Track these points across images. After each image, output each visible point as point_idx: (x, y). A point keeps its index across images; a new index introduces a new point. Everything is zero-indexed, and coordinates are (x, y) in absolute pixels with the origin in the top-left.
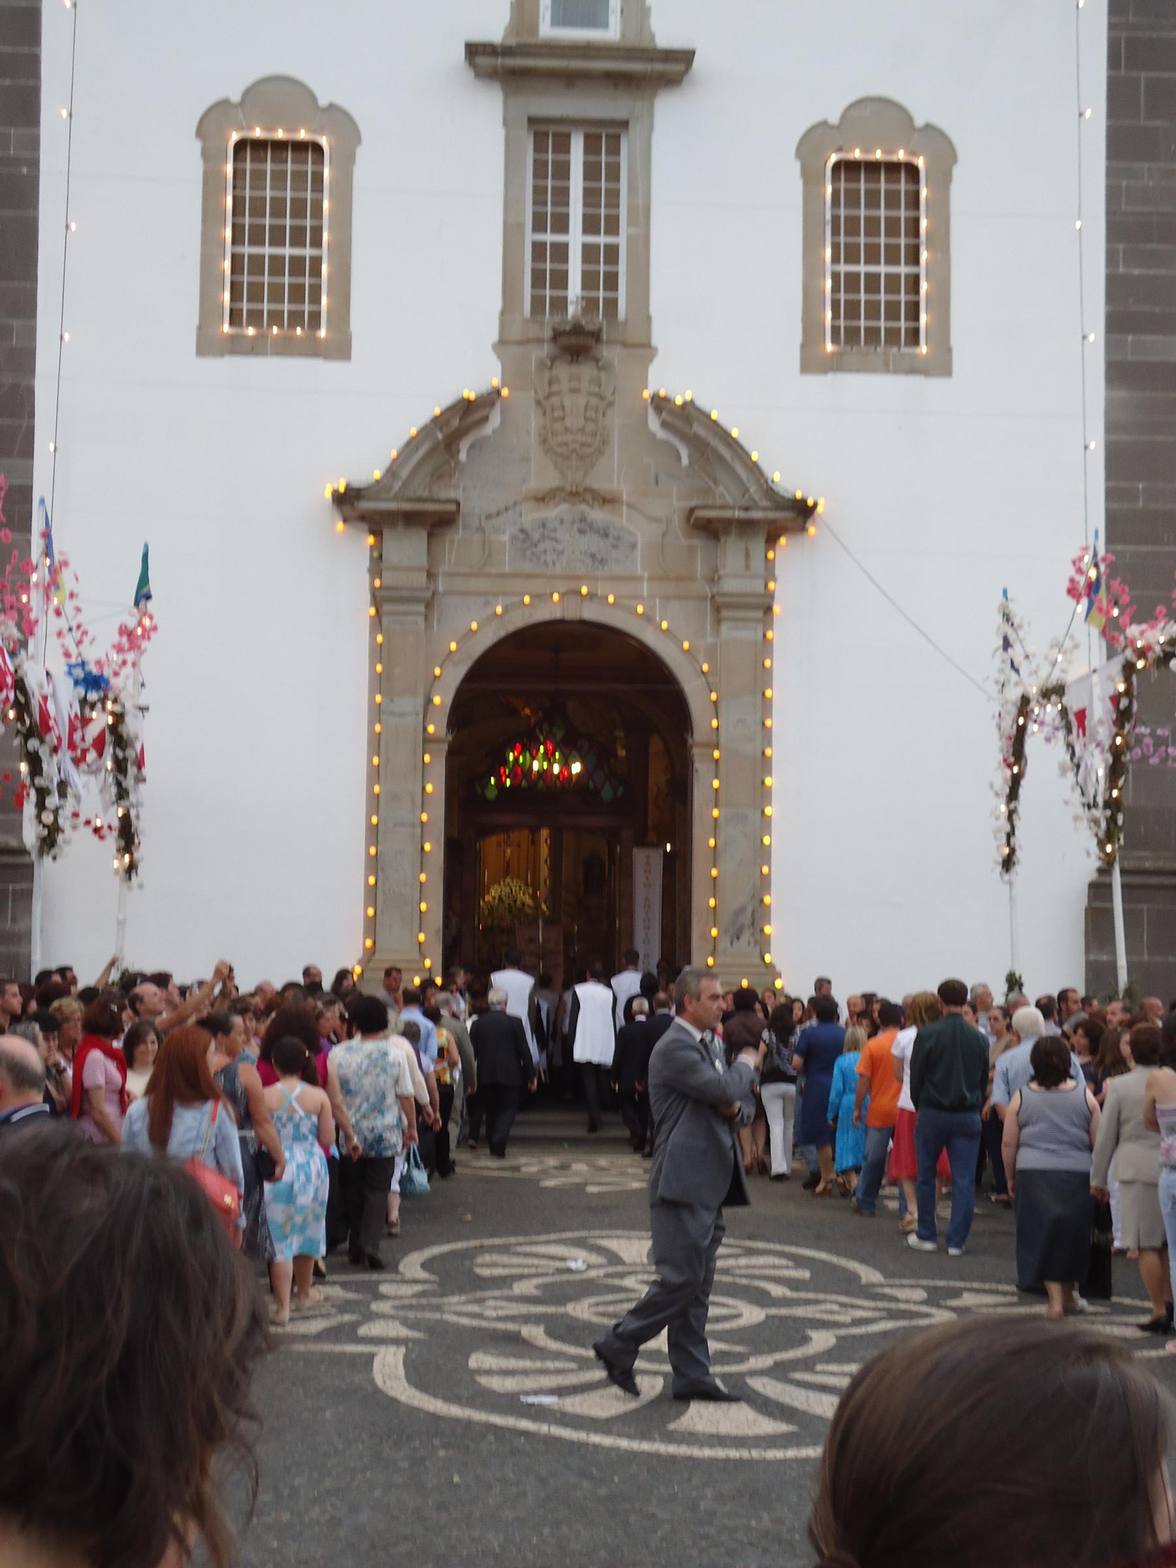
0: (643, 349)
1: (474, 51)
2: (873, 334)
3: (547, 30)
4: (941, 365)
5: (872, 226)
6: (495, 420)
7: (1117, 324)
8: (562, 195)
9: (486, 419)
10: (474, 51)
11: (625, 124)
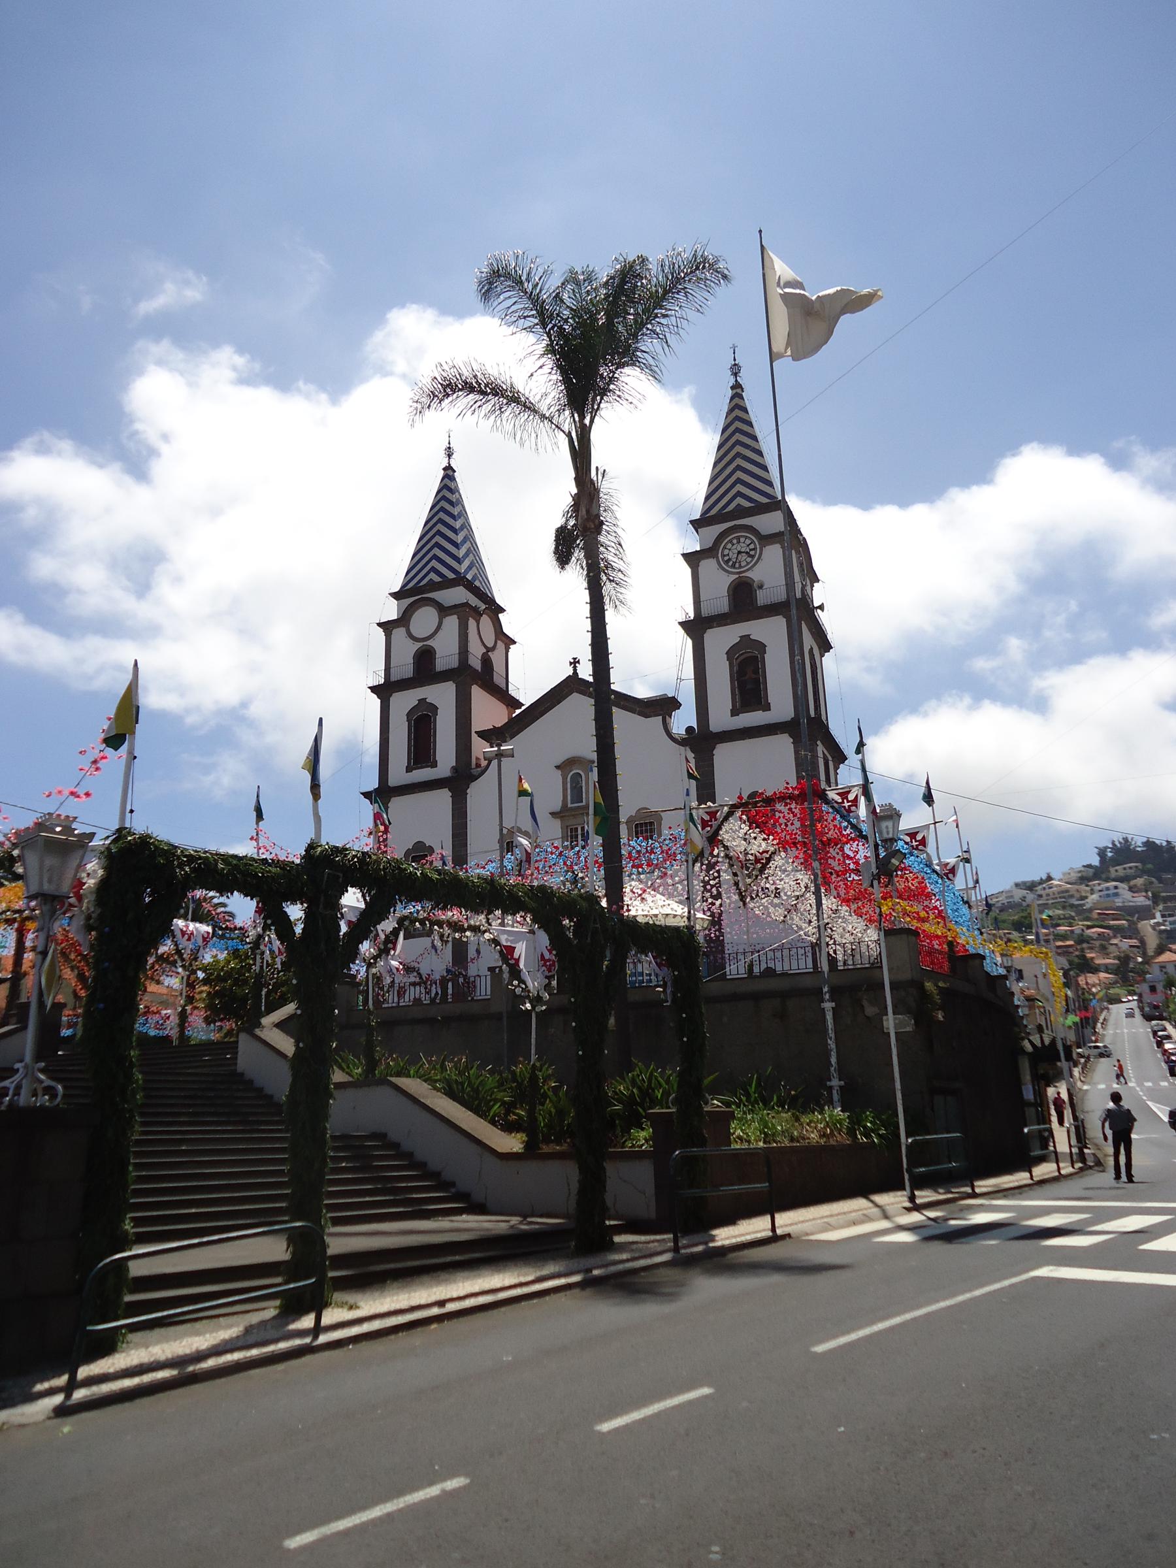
1: (552, 814)
3: (569, 805)
10: (552, 814)
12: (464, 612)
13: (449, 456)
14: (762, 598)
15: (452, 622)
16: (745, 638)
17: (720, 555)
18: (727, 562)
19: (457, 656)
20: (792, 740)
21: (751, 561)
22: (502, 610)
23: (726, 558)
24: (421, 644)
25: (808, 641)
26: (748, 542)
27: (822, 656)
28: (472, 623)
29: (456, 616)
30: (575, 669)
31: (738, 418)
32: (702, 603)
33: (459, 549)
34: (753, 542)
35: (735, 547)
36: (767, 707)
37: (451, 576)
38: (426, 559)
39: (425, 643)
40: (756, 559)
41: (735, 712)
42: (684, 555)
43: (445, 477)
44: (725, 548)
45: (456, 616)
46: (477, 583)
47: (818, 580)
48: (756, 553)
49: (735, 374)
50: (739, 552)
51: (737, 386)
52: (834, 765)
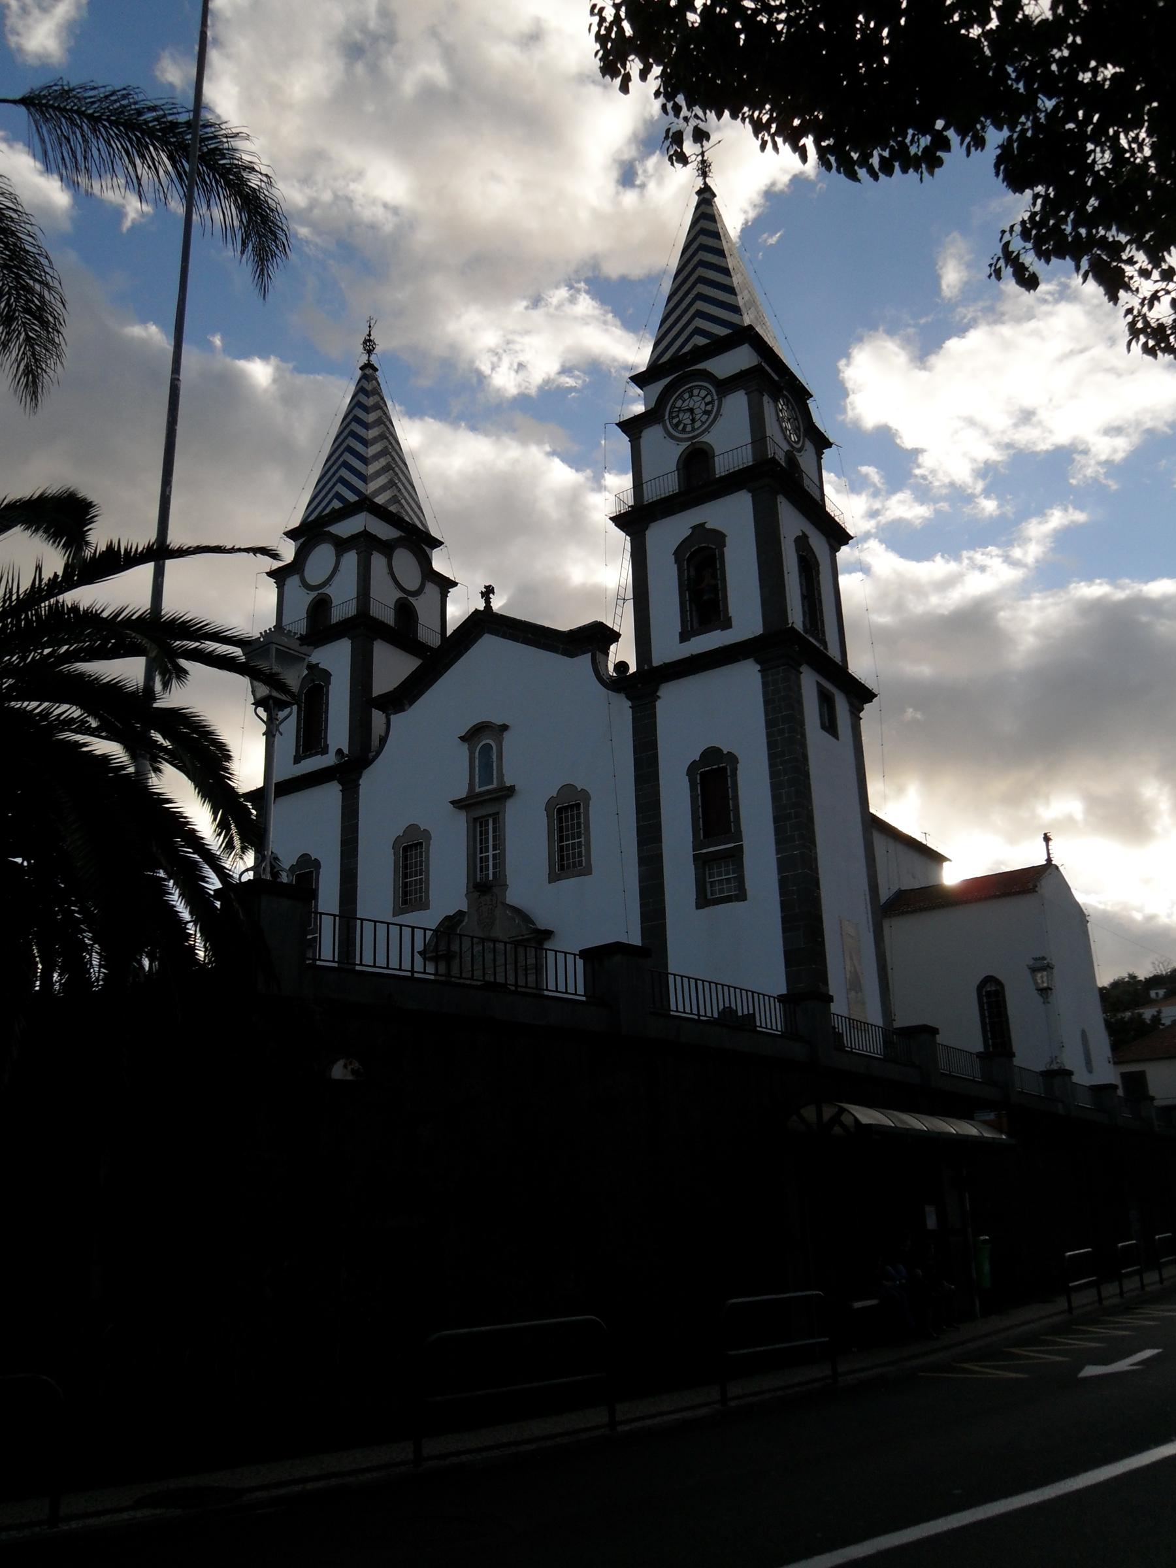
0: (505, 886)
2: (574, 863)
3: (478, 790)
4: (587, 871)
5: (573, 825)
6: (466, 920)
7: (641, 843)
8: (487, 839)
9: (462, 921)
11: (498, 813)
12: (365, 543)
13: (369, 352)
14: (723, 466)
15: (351, 559)
16: (699, 529)
17: (666, 417)
18: (676, 426)
19: (355, 601)
20: (759, 667)
22: (436, 543)
23: (675, 421)
24: (316, 593)
25: (791, 523)
26: (703, 393)
27: (835, 549)
28: (378, 562)
29: (355, 551)
30: (488, 602)
31: (703, 232)
32: (644, 485)
33: (366, 465)
35: (687, 402)
36: (726, 624)
37: (352, 498)
38: (331, 484)
39: (320, 591)
41: (684, 637)
42: (620, 425)
43: (364, 377)
44: (673, 406)
45: (355, 551)
46: (393, 508)
47: (828, 444)
48: (713, 406)
50: (691, 410)
52: (851, 704)
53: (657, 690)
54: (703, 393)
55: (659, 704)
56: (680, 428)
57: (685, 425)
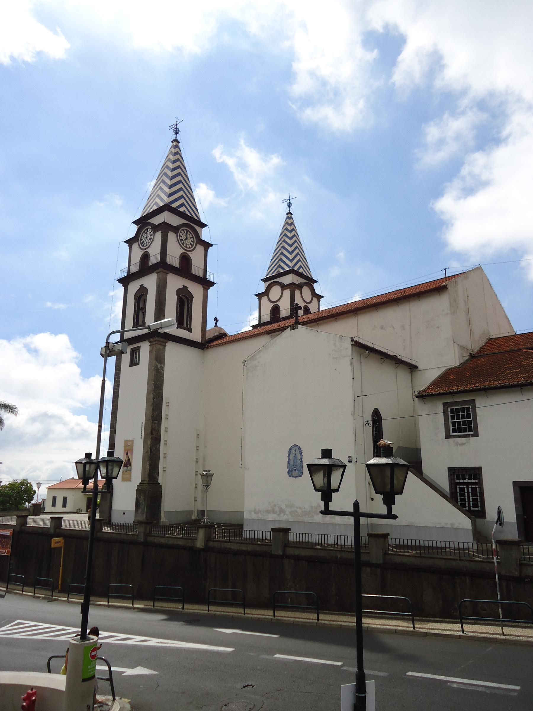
16: (185, 288)
17: (179, 234)
21: (191, 248)
23: (181, 238)
34: (193, 237)
36: (190, 330)
40: (194, 247)
49: (176, 134)
50: (187, 239)
51: (176, 140)
53: (166, 343)
54: (191, 237)
55: (166, 347)
56: (182, 242)
57: (184, 242)
